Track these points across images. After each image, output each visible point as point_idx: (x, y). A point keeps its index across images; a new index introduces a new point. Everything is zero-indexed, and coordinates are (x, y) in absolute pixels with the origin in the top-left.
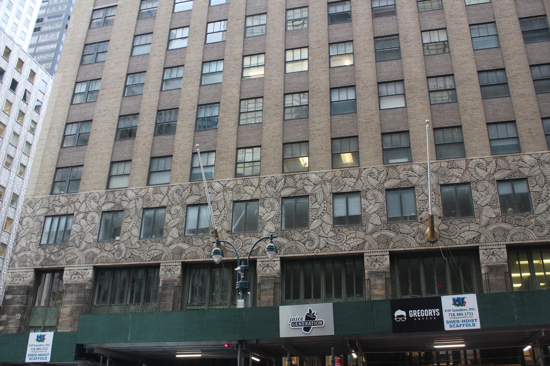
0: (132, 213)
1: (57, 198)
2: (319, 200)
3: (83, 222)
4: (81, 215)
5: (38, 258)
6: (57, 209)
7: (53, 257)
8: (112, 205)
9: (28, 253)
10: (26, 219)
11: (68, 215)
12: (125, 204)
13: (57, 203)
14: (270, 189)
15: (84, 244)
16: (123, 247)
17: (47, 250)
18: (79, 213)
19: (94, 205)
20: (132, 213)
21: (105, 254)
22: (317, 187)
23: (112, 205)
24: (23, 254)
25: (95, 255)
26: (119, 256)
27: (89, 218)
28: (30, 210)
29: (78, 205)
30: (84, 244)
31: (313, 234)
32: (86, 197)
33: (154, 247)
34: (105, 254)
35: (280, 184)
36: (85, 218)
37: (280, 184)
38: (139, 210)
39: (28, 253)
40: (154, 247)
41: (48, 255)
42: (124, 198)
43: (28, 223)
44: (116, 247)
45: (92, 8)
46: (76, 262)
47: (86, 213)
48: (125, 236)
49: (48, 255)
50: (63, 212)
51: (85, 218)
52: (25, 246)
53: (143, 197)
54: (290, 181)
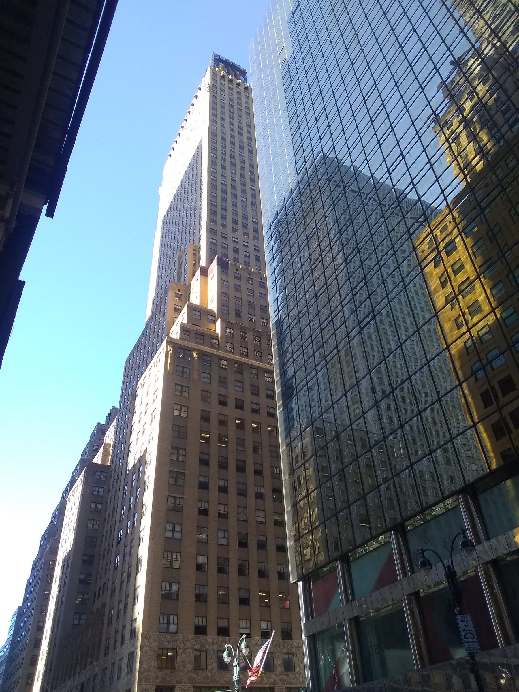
0: (212, 653)
1: (164, 636)
2: (298, 656)
3: (183, 655)
4: (182, 651)
5: (157, 677)
6: (166, 644)
7: (167, 677)
8: (199, 646)
9: (149, 673)
10: (144, 648)
11: (172, 649)
12: (207, 646)
13: (164, 639)
14: (278, 648)
15: (186, 670)
16: (210, 675)
17: (163, 672)
18: (180, 649)
19: (189, 645)
20: (212, 653)
21: (199, 678)
22: (297, 650)
23: (199, 646)
24: (146, 674)
25: (194, 679)
26: (207, 680)
27: (186, 653)
28: (147, 643)
29: (179, 643)
30: (186, 670)
31: (297, 676)
32: (183, 637)
33: (226, 676)
34: (199, 678)
35: (282, 645)
36: (184, 652)
37: (282, 645)
38: (215, 651)
39: (149, 673)
40: (226, 676)
41: (164, 676)
42: (206, 642)
43: (146, 651)
44: (205, 673)
45: (167, 494)
46: (183, 681)
47: (185, 649)
48: (209, 668)
49: (164, 676)
50: (170, 646)
51: (184, 652)
52: (147, 668)
53: (217, 643)
54: (285, 644)
